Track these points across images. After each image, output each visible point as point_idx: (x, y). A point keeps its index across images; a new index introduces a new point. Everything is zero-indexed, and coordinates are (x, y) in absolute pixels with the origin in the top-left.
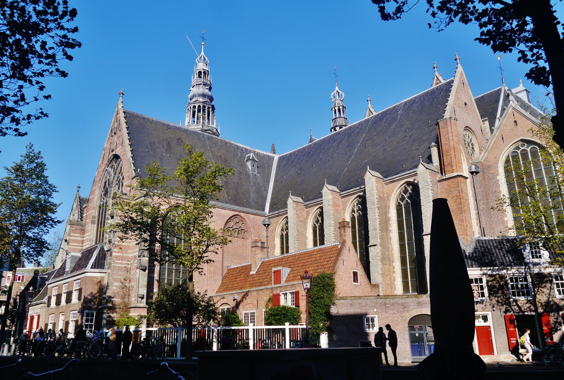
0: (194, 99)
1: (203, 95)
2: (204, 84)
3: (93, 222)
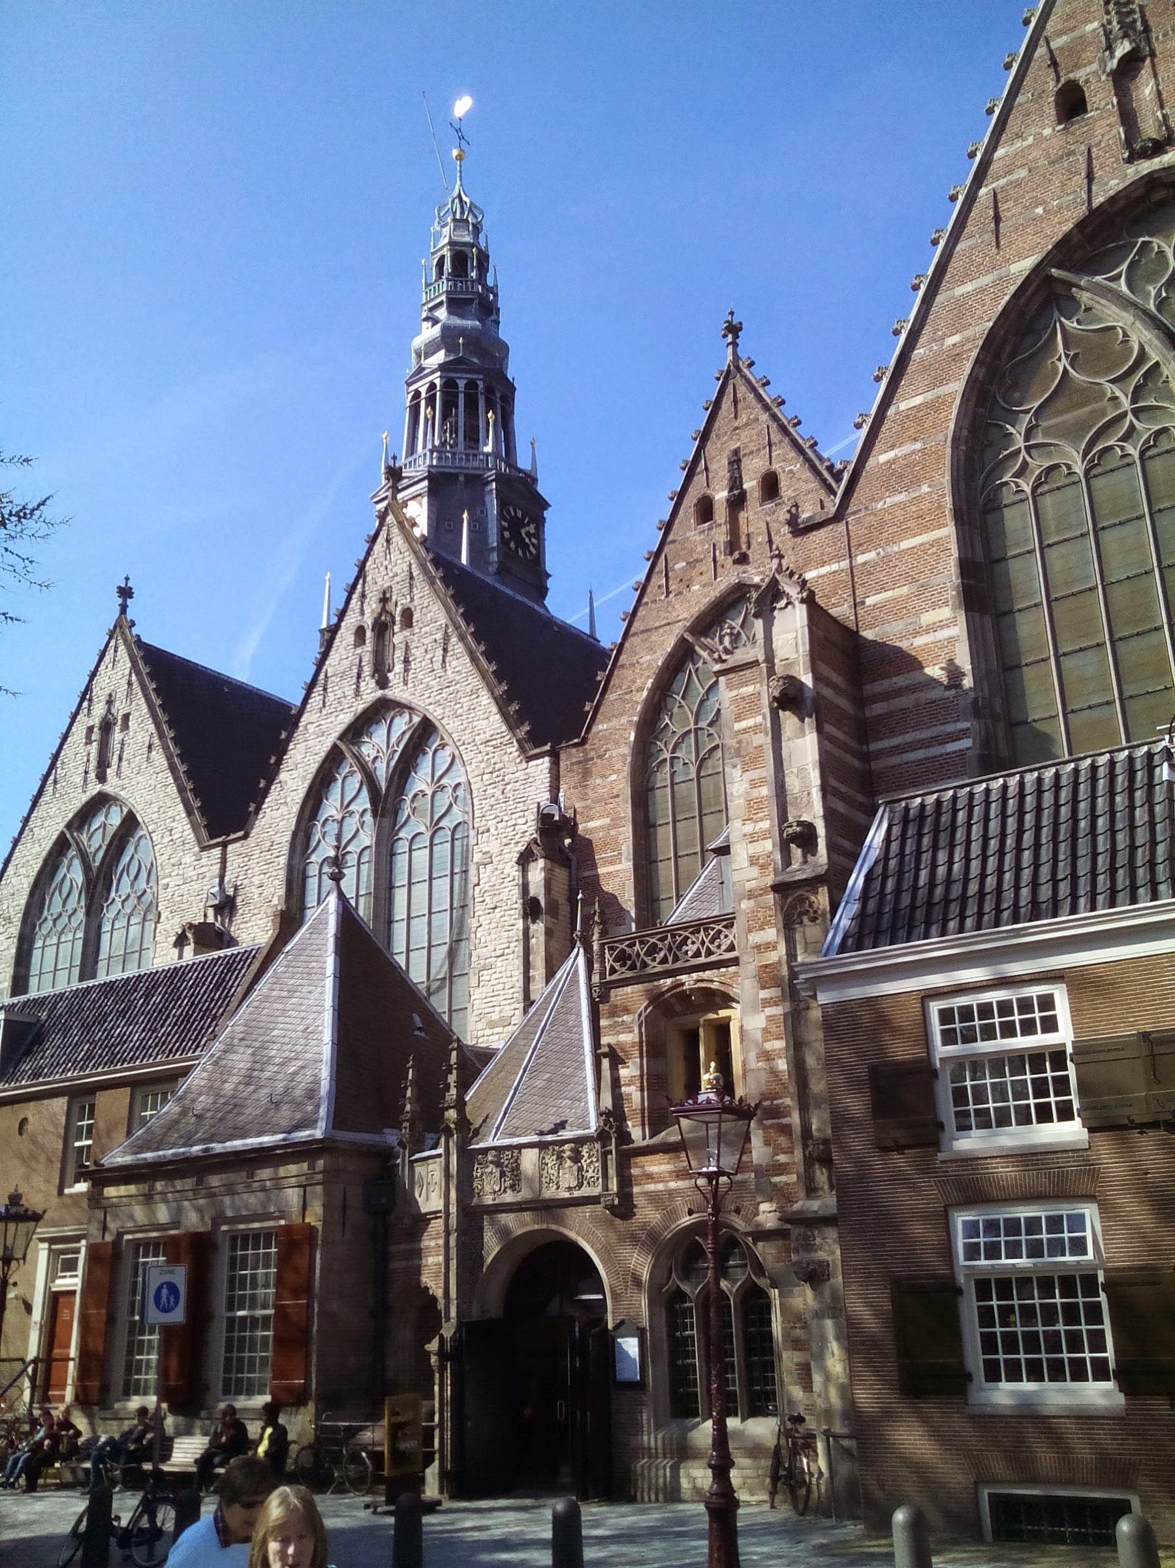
2: (480, 304)
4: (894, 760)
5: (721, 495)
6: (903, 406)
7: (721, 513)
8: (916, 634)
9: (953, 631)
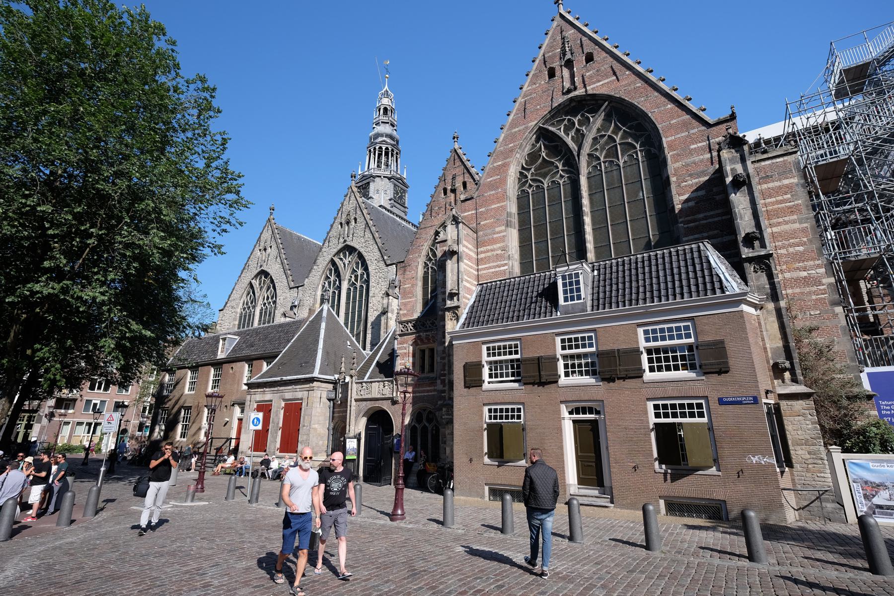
0: (380, 139)
1: (391, 137)
3: (508, 224)
4: (485, 272)
5: (449, 188)
6: (495, 165)
7: (448, 191)
8: (494, 234)
9: (504, 234)
